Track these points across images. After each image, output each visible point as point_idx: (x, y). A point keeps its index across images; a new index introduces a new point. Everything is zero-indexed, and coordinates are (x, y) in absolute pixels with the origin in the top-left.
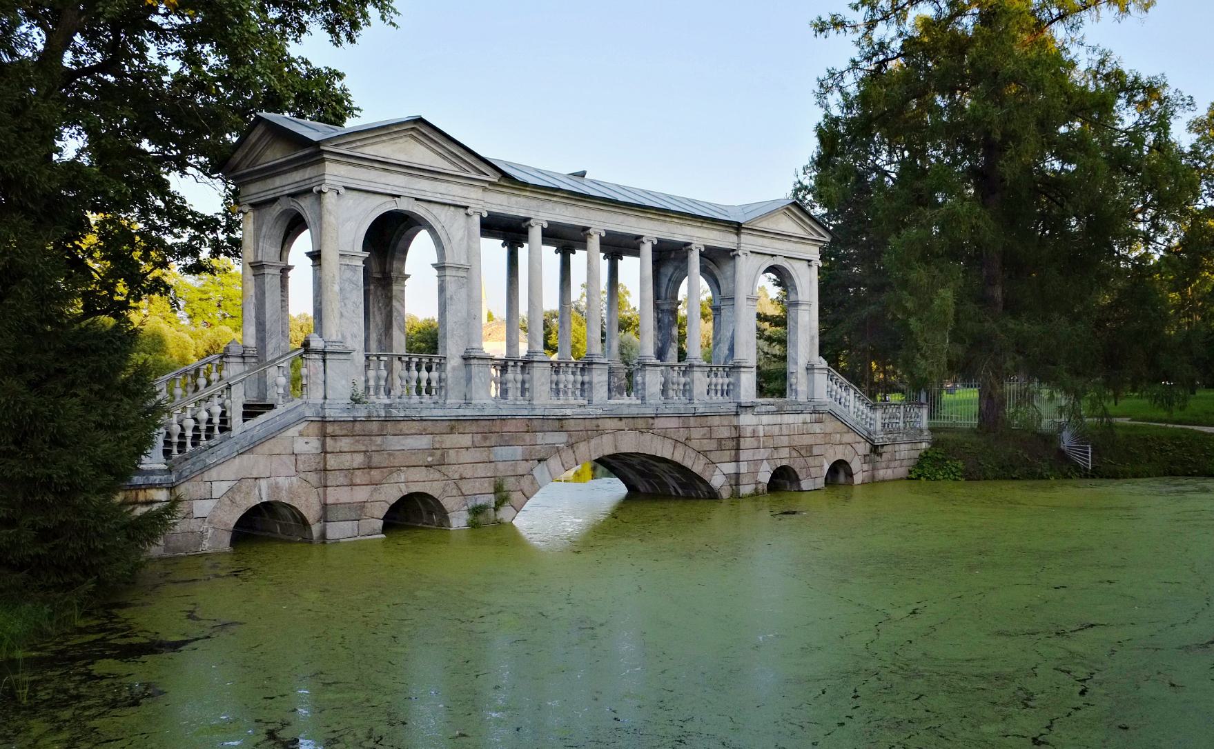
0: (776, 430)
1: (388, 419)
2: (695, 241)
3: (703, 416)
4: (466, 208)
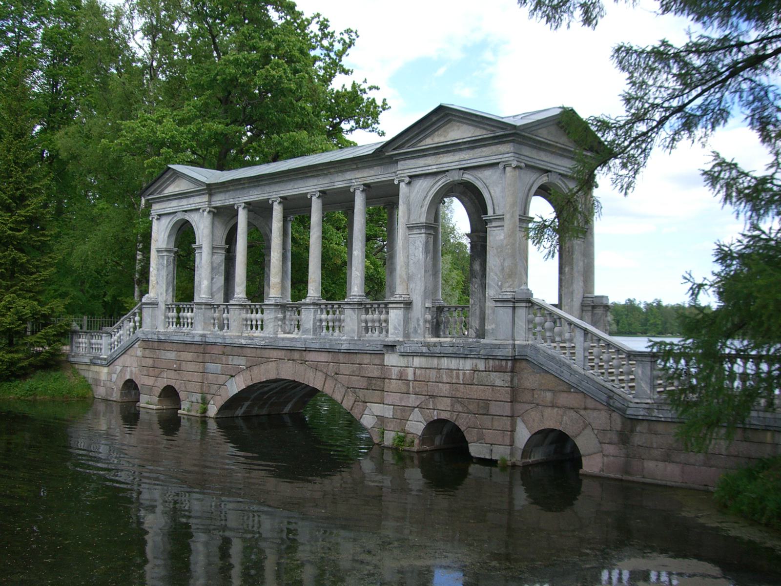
0: (433, 374)
1: (160, 341)
2: (355, 183)
3: (348, 353)
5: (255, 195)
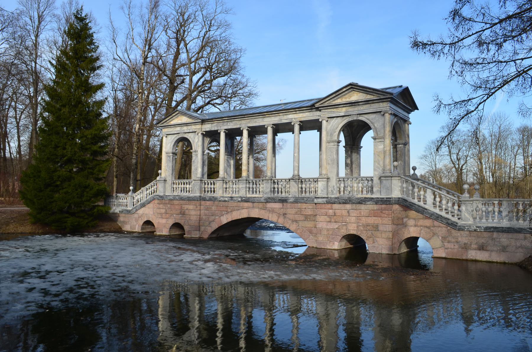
4: (195, 132)
5: (232, 125)
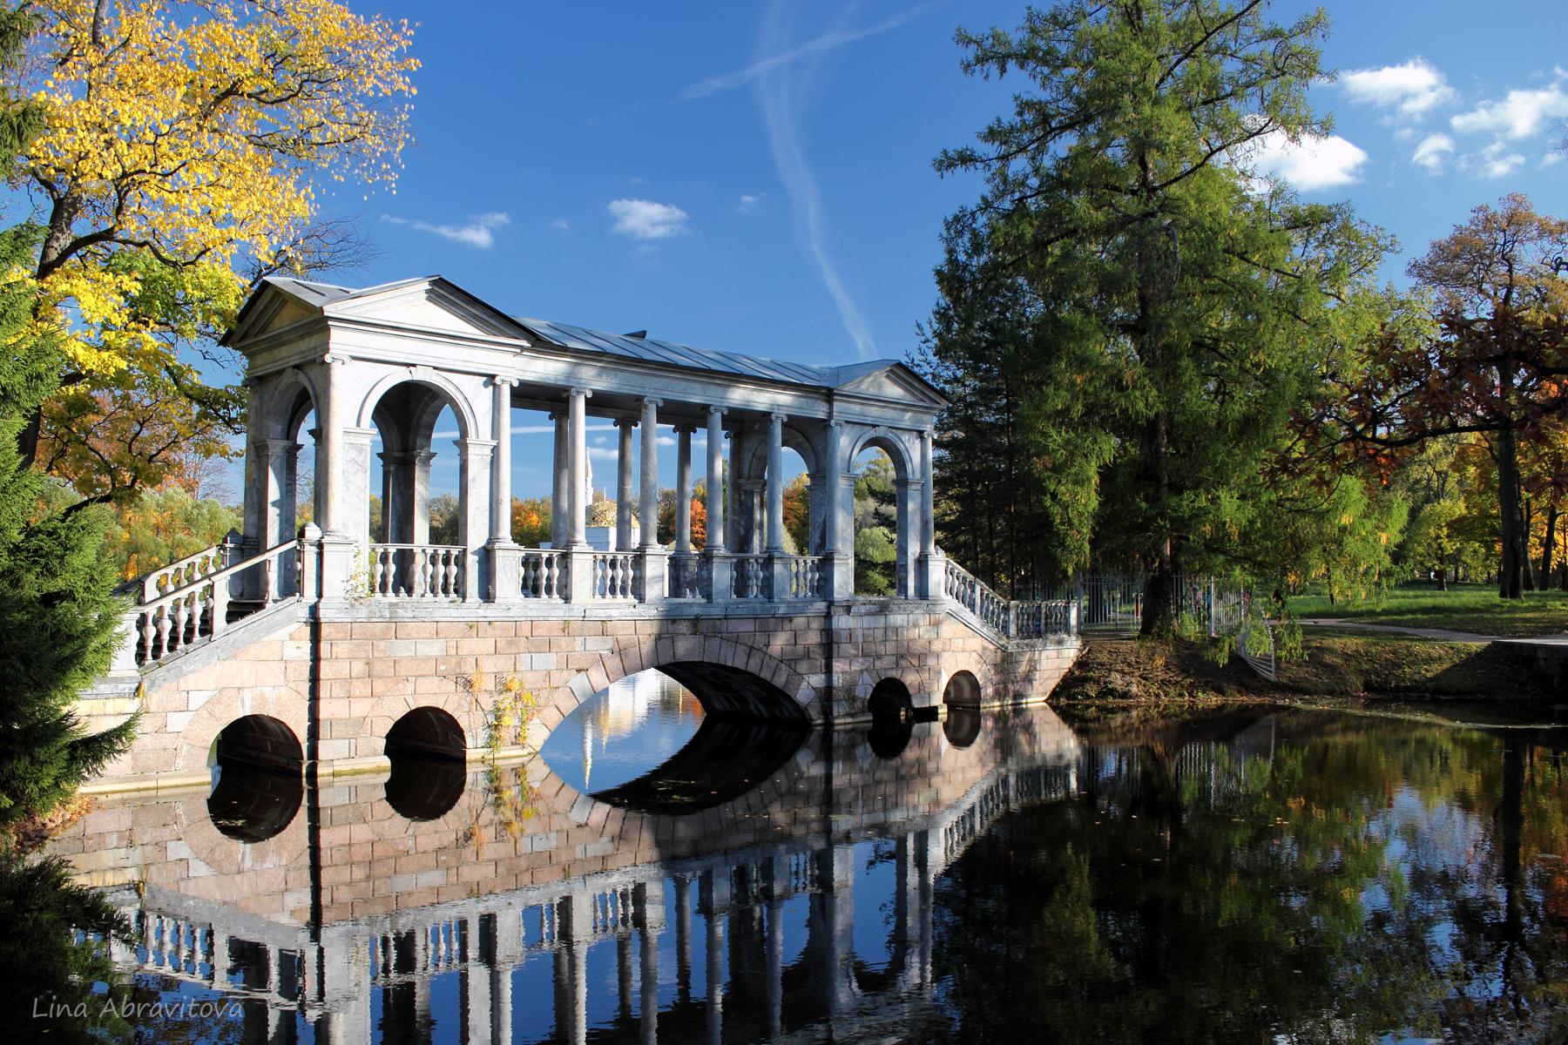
4: (493, 377)
